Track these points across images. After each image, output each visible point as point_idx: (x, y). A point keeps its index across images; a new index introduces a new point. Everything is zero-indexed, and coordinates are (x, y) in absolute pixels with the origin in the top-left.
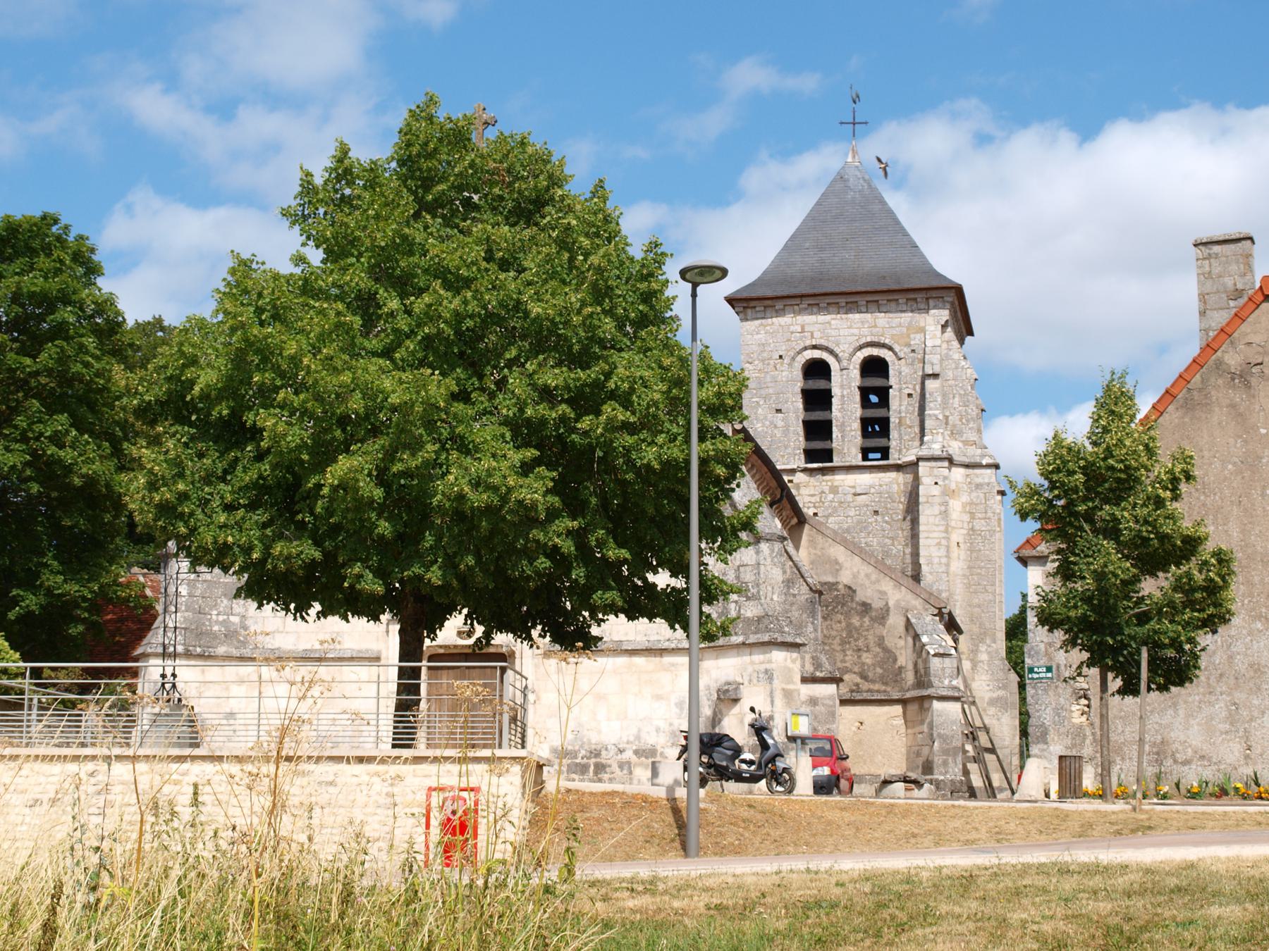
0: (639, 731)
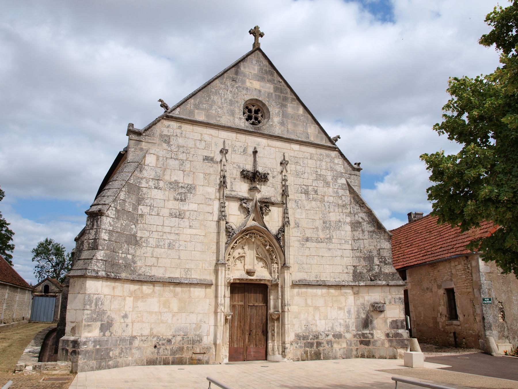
0: (333, 325)
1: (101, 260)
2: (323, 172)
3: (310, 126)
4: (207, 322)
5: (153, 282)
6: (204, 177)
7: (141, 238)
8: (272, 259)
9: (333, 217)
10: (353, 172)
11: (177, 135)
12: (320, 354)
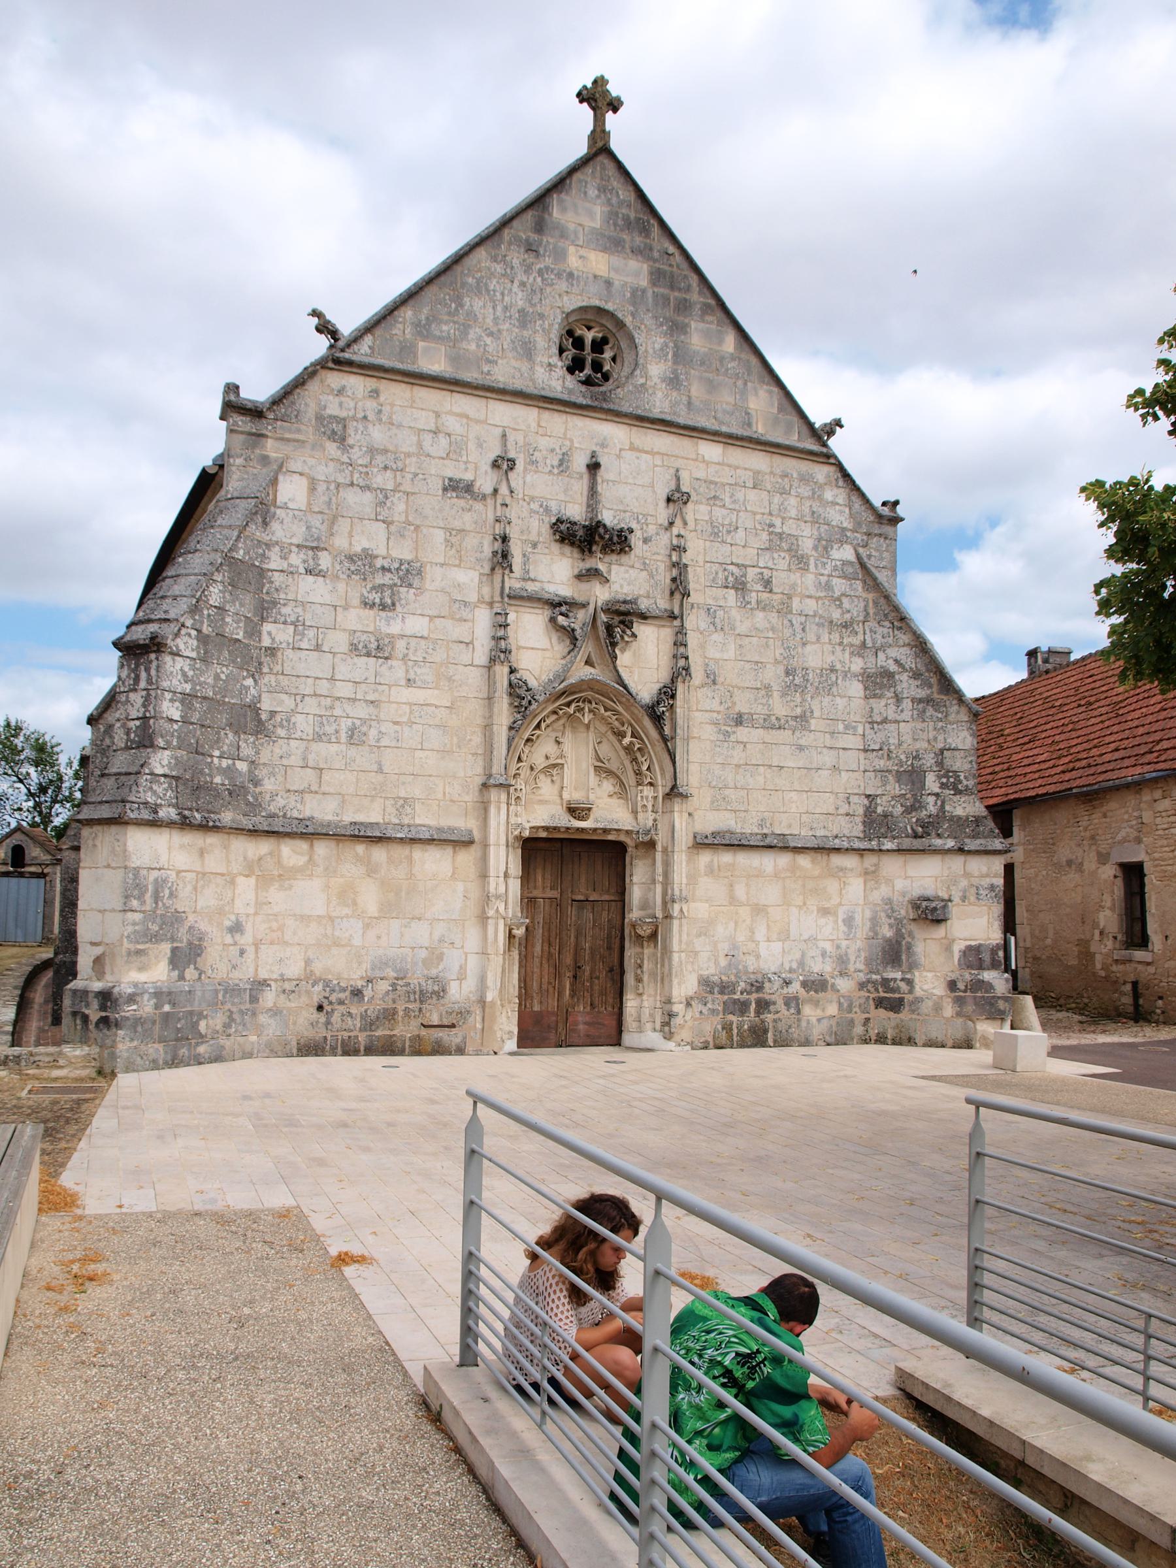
0: (803, 956)
1: (165, 776)
2: (790, 528)
3: (755, 389)
4: (458, 944)
5: (307, 832)
6: (447, 541)
7: (273, 714)
8: (638, 773)
9: (815, 656)
10: (876, 529)
11: (365, 417)
12: (766, 1031)
